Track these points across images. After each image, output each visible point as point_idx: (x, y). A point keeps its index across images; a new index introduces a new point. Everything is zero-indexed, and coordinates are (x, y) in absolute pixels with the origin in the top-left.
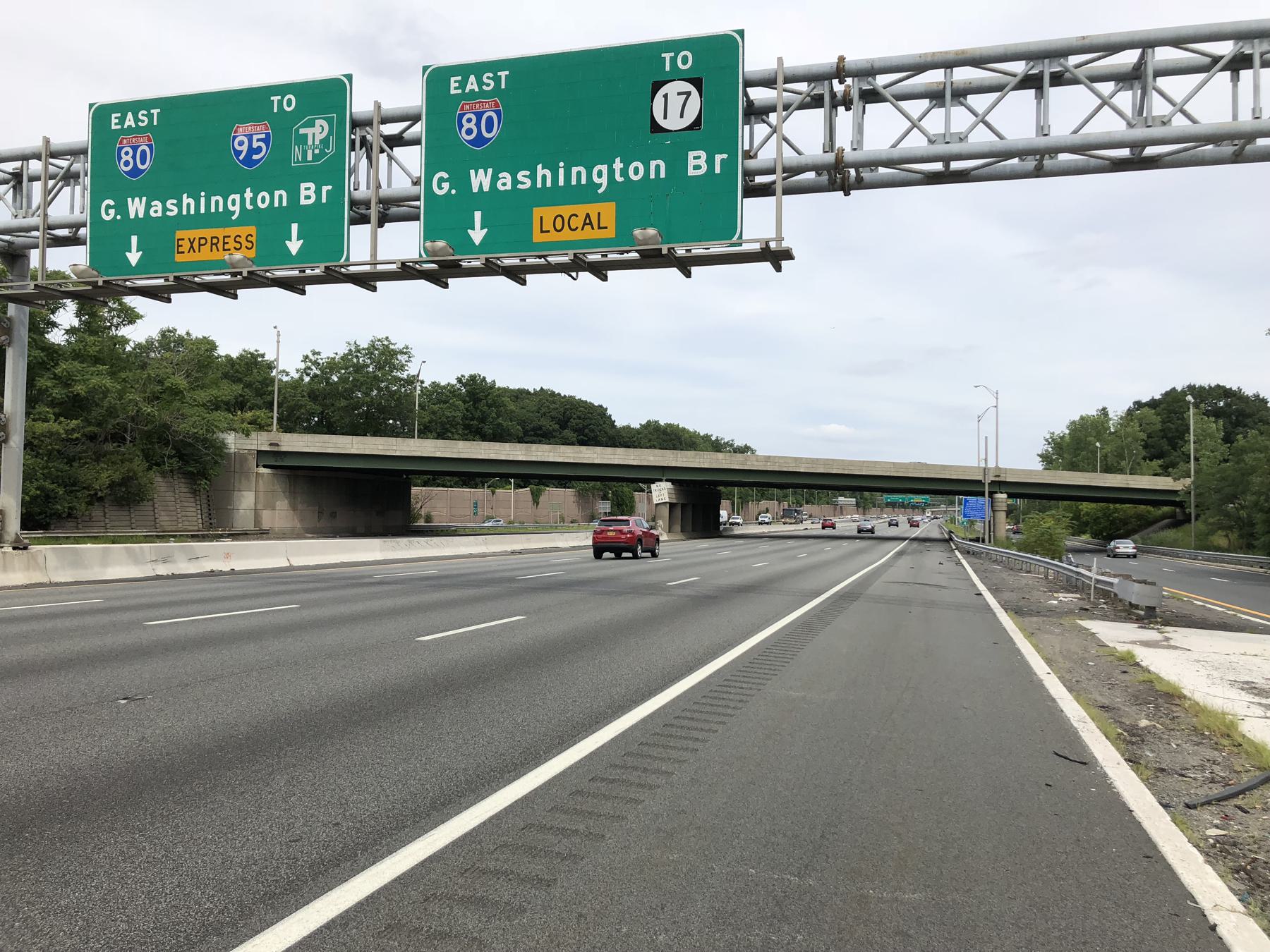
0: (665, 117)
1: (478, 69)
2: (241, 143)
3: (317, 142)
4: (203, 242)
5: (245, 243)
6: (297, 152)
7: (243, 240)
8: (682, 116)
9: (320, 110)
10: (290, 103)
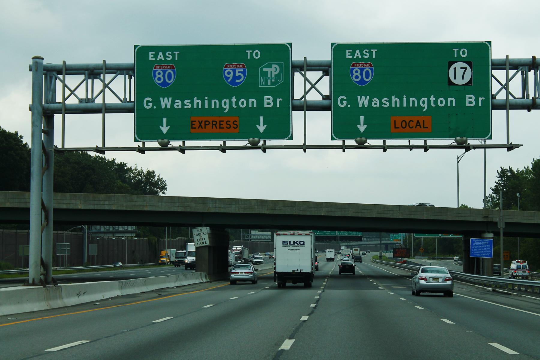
0: (455, 78)
1: (361, 47)
2: (229, 73)
3: (273, 76)
4: (207, 123)
5: (232, 125)
6: (262, 80)
7: (231, 123)
8: (463, 79)
9: (275, 60)
10: (257, 55)
